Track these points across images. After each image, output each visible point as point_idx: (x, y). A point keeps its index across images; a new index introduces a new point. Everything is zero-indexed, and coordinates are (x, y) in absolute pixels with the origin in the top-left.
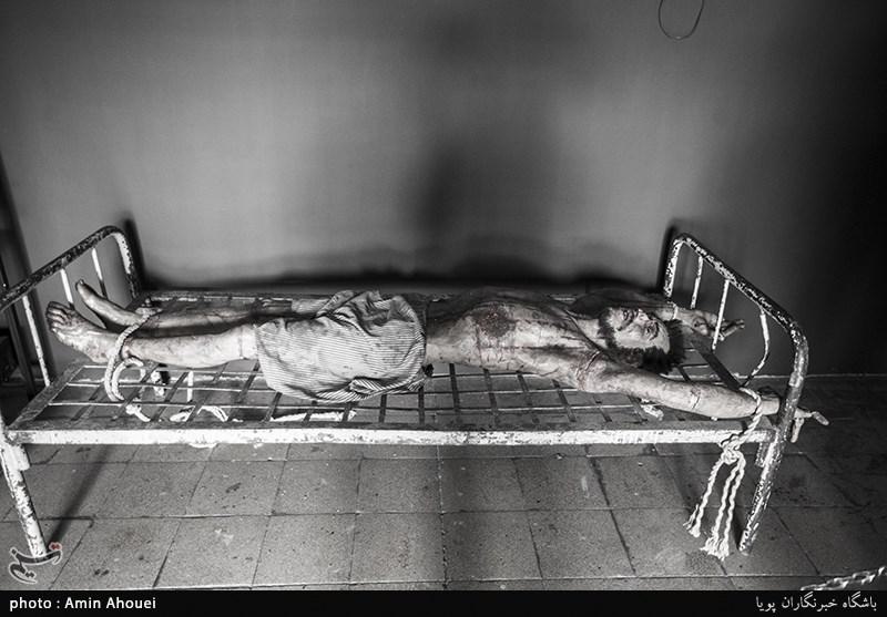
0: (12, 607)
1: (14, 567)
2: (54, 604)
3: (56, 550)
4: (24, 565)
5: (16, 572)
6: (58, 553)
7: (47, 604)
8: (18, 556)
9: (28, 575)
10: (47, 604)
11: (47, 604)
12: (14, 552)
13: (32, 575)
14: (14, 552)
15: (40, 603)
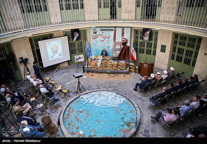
0: (3, 142)
1: (3, 132)
2: (11, 141)
3: (13, 128)
4: (4, 131)
5: (4, 133)
6: (13, 129)
7: (9, 141)
8: (4, 130)
9: (6, 134)
10: (10, 141)
11: (10, 141)
12: (3, 129)
13: (7, 134)
14: (3, 129)
15: (9, 141)
